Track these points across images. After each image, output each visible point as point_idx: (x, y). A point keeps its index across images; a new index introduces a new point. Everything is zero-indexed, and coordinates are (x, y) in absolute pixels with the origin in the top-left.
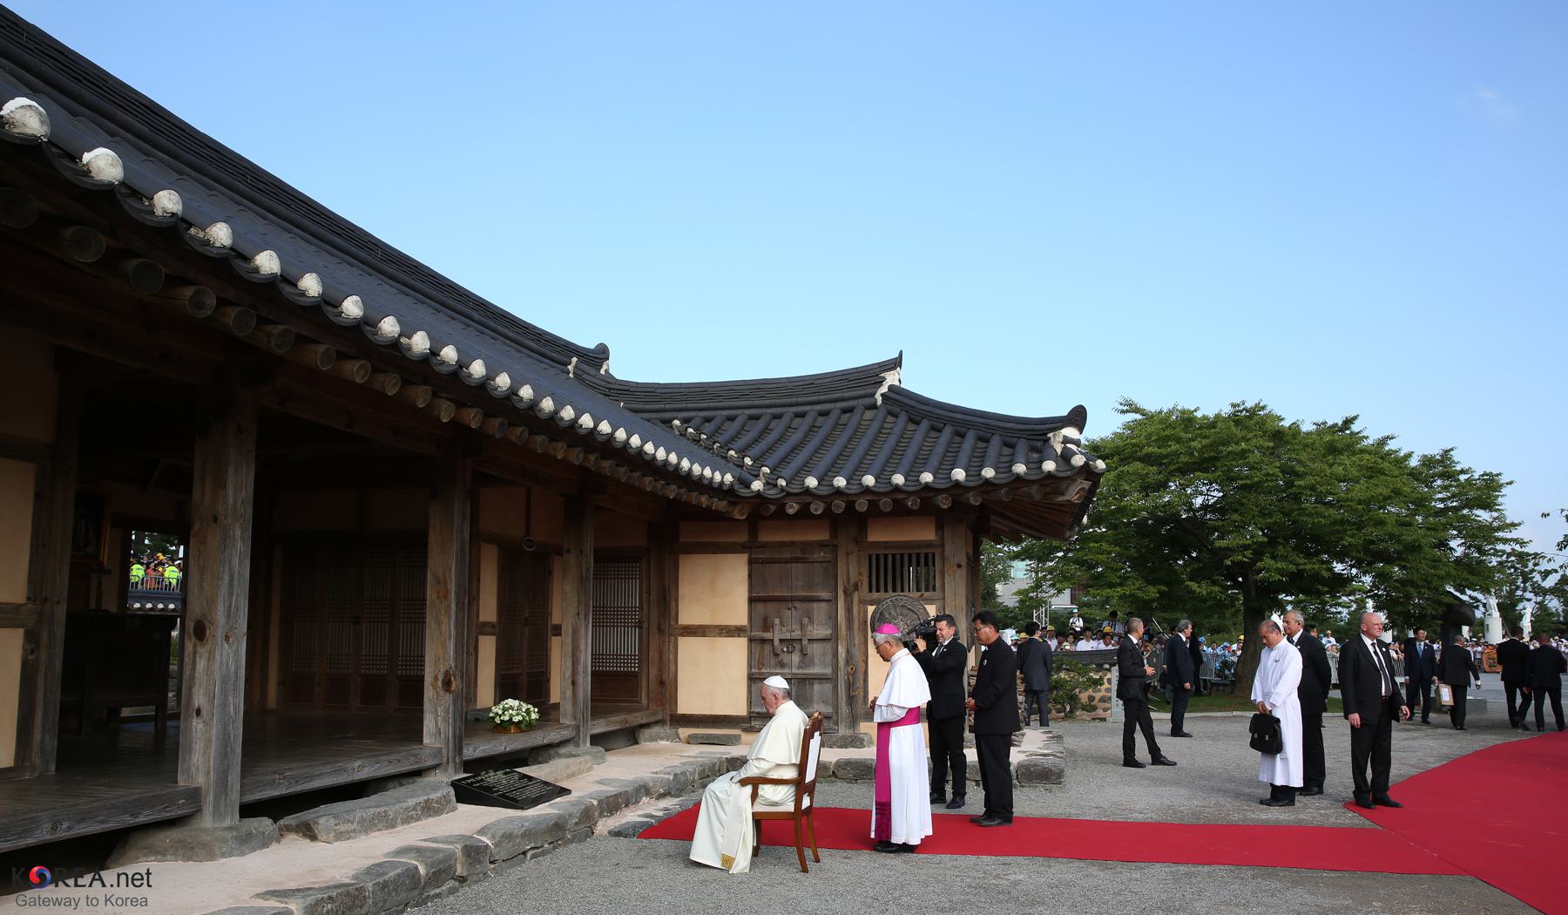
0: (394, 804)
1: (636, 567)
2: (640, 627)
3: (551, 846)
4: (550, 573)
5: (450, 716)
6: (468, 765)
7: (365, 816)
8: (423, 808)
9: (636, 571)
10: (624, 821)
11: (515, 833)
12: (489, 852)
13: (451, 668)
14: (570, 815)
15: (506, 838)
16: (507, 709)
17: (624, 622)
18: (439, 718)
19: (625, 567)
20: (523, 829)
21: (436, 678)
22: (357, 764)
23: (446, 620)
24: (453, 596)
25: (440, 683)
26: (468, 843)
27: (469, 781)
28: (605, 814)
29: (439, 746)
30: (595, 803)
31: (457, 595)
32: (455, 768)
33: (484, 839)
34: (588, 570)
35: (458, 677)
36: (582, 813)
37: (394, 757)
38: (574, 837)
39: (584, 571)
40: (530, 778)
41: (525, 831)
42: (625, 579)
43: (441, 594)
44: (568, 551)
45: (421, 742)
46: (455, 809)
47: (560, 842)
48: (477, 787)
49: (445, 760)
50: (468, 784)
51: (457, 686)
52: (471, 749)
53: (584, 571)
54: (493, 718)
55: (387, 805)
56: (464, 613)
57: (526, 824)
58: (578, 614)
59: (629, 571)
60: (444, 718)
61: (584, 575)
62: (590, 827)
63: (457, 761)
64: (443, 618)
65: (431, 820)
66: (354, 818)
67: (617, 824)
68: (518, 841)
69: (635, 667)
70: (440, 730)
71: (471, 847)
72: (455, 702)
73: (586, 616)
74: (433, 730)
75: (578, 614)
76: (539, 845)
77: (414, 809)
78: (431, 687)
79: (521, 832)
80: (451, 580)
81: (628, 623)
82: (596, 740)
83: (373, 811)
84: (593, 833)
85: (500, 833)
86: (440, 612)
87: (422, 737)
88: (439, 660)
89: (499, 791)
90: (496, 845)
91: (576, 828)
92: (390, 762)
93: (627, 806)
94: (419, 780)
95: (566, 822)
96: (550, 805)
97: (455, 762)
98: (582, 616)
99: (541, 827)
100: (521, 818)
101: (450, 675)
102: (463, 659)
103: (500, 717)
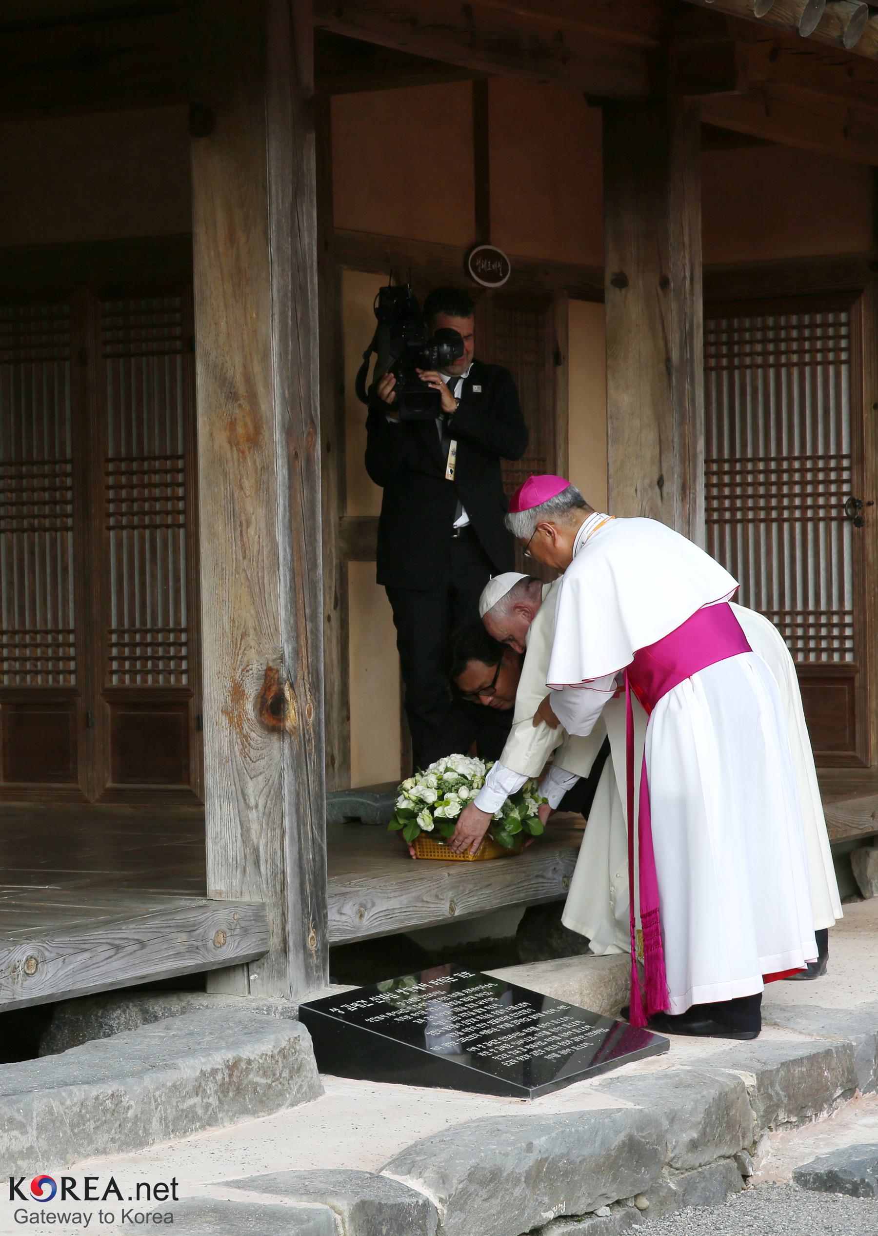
0: (138, 1074)
1: (837, 325)
2: (858, 522)
3: (619, 1213)
4: (559, 359)
5: (287, 806)
7: (55, 1104)
8: (223, 1089)
9: (837, 337)
10: (845, 1140)
11: (509, 1166)
12: (431, 1225)
13: (282, 658)
14: (673, 1118)
15: (483, 1183)
16: (454, 788)
17: (804, 508)
18: (253, 815)
19: (800, 327)
20: (531, 1160)
21: (237, 693)
22: (22, 952)
23: (261, 512)
24: (278, 436)
25: (249, 707)
26: (369, 1195)
27: (353, 1007)
28: (782, 1116)
29: (257, 899)
30: (750, 1080)
31: (289, 431)
32: (308, 969)
33: (414, 1183)
34: (687, 338)
35: (304, 688)
36: (708, 1113)
37: (129, 931)
38: (688, 1187)
39: (675, 338)
40: (536, 1001)
41: (540, 1163)
42: (801, 365)
43: (240, 431)
44: (621, 281)
45: (199, 887)
46: (314, 1092)
47: (644, 1202)
49: (274, 942)
50: (348, 1015)
51: (300, 714)
52: (350, 909)
53: (675, 338)
54: (411, 815)
55: (119, 1076)
56: (313, 489)
57: (541, 1142)
58: (660, 483)
59: (813, 338)
60: (268, 815)
61: (675, 356)
62: (736, 1157)
63: (313, 945)
65: (247, 1123)
66: (28, 1113)
67: (824, 1151)
68: (517, 1192)
69: (842, 651)
70: (256, 850)
71: (380, 1208)
72: (298, 766)
73: (685, 489)
74: (236, 849)
75: (660, 483)
76: (580, 1209)
77: (198, 1090)
78: (224, 721)
79: (523, 1168)
80: (268, 385)
81: (816, 507)
83: (79, 1093)
84: (745, 1177)
85: (460, 1169)
86: (241, 488)
87: (203, 874)
88: (244, 635)
90: (456, 1203)
91: (693, 1159)
92: (118, 948)
93: (849, 1092)
94: (198, 1000)
95: (661, 1138)
96: (609, 1085)
97: (305, 947)
98: (673, 487)
99: (586, 1152)
100: (523, 1122)
101: (280, 683)
102: (315, 632)
103: (432, 809)
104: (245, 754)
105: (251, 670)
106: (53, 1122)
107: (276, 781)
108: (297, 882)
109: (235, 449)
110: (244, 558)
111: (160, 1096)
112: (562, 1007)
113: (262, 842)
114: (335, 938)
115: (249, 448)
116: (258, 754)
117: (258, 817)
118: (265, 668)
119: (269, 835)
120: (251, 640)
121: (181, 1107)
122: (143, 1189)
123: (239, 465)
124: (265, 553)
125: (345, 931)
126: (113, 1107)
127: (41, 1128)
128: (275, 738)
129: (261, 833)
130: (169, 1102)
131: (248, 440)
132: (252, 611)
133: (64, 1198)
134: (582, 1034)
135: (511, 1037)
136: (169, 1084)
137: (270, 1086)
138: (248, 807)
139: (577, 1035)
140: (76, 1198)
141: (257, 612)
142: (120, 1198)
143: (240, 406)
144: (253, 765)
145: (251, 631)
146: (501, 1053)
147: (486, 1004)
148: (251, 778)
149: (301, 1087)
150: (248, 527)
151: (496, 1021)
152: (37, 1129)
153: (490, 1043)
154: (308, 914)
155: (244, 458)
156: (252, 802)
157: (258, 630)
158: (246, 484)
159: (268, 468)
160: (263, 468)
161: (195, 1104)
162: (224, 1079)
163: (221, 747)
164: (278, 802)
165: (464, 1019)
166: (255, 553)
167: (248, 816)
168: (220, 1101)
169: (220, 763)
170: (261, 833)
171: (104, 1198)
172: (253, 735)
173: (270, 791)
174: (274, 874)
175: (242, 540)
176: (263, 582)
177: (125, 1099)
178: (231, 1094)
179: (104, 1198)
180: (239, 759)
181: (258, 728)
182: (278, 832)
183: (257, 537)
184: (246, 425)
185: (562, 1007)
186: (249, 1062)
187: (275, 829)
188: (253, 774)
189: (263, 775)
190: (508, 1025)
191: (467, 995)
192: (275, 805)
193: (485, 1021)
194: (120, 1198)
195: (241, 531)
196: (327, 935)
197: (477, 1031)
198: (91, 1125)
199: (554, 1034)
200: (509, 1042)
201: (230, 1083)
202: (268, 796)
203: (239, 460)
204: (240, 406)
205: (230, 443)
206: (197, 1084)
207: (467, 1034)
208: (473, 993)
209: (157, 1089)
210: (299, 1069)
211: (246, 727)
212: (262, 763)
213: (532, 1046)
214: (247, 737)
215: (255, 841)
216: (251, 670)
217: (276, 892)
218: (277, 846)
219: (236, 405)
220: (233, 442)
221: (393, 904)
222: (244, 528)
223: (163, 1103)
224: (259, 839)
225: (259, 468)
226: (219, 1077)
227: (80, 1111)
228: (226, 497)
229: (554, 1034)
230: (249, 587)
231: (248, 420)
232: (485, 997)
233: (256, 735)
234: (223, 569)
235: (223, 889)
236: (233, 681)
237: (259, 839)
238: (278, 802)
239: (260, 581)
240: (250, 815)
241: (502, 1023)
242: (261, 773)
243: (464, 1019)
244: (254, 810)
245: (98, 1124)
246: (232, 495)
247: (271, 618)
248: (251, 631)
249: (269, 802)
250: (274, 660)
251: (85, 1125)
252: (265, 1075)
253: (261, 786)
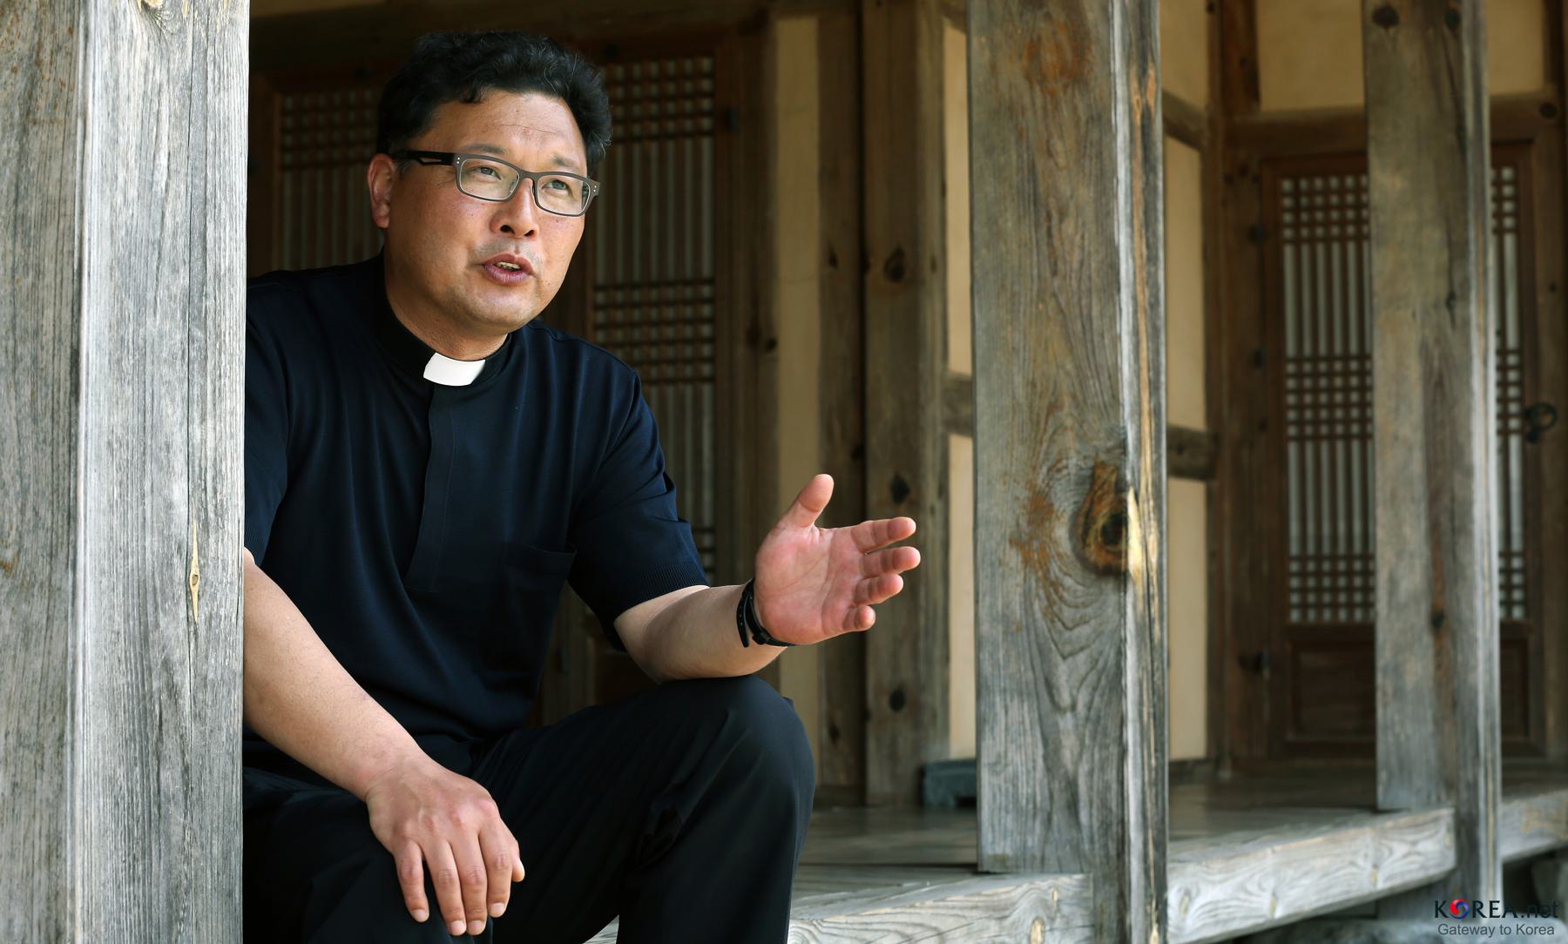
18: (1066, 722)
23: (1086, 194)
25: (1061, 531)
43: (1048, 57)
64: (1065, 189)
70: (1072, 785)
86: (1050, 153)
88: (1054, 407)
104: (1052, 615)
105: (1066, 467)
107: (1112, 661)
109: (1037, 88)
110: (1054, 273)
113: (1084, 769)
115: (1066, 87)
116: (1078, 616)
117: (1076, 726)
118: (1090, 463)
119: (1097, 756)
120: (1067, 416)
123: (1046, 116)
124: (1093, 265)
129: (1081, 754)
131: (1062, 73)
132: (1069, 366)
138: (1057, 707)
141: (1078, 368)
143: (1048, 16)
144: (1067, 634)
145: (1067, 401)
148: (1064, 658)
150: (1061, 221)
154: (1151, 896)
155: (1056, 107)
156: (1065, 699)
157: (1080, 397)
158: (1059, 146)
159: (1100, 117)
160: (1090, 119)
163: (1007, 605)
164: (1114, 699)
166: (1076, 266)
167: (1056, 724)
169: (1005, 633)
170: (1081, 754)
172: (1068, 582)
173: (1099, 680)
174: (1105, 826)
175: (1050, 244)
176: (1090, 315)
180: (1042, 624)
181: (1077, 569)
182: (1114, 750)
183: (1078, 238)
184: (1058, 48)
187: (1107, 747)
188: (1067, 649)
189: (1087, 651)
192: (1109, 703)
195: (1049, 229)
202: (1095, 689)
203: (1045, 109)
204: (1048, 16)
205: (1028, 77)
211: (1055, 568)
212: (1084, 631)
214: (1055, 585)
215: (1070, 767)
216: (1066, 467)
217: (1107, 856)
218: (1112, 775)
219: (1040, 14)
220: (1035, 75)
222: (1055, 221)
224: (1076, 764)
225: (1083, 119)
228: (1020, 169)
230: (1065, 325)
231: (1063, 38)
233: (1073, 583)
234: (1013, 295)
235: (1009, 852)
236: (1031, 485)
237: (1076, 764)
238: (1114, 699)
239: (1085, 312)
240: (1062, 724)
242: (1082, 649)
244: (1069, 715)
246: (1032, 168)
247: (1104, 377)
248: (1067, 401)
249: (1097, 699)
250: (1109, 451)
253: (1083, 671)
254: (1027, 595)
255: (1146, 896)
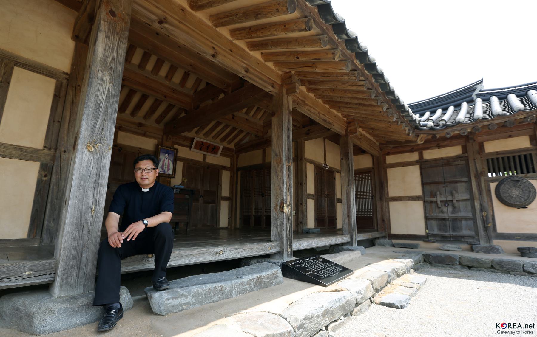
6: (296, 253)
18: (278, 227)
21: (277, 205)
23: (281, 174)
25: (278, 208)
48: (297, 268)
51: (288, 209)
60: (281, 227)
70: (279, 233)
74: (275, 233)
77: (248, 283)
78: (274, 210)
80: (283, 153)
82: (360, 243)
86: (278, 170)
88: (278, 195)
89: (310, 271)
97: (287, 251)
104: (277, 216)
106: (199, 294)
108: (286, 239)
111: (236, 286)
112: (334, 264)
113: (280, 231)
114: (293, 250)
121: (242, 288)
122: (527, 326)
125: (297, 248)
126: (220, 289)
127: (193, 296)
128: (282, 213)
130: (239, 287)
133: (508, 328)
134: (338, 270)
135: (324, 271)
136: (239, 283)
137: (269, 282)
138: (278, 225)
139: (337, 270)
140: (511, 328)
142: (521, 328)
146: (321, 274)
147: (320, 263)
149: (277, 281)
151: (321, 267)
152: (192, 296)
153: (319, 272)
156: (278, 225)
158: (279, 170)
161: (247, 287)
162: (256, 281)
165: (315, 266)
168: (254, 286)
171: (518, 328)
174: (282, 237)
177: (225, 287)
178: (258, 284)
179: (518, 328)
180: (277, 217)
185: (334, 264)
186: (264, 276)
190: (324, 268)
191: (317, 261)
193: (319, 267)
194: (521, 328)
196: (292, 249)
197: (317, 269)
198: (212, 294)
199: (333, 270)
200: (323, 272)
201: (258, 281)
206: (248, 282)
207: (315, 270)
208: (318, 261)
209: (236, 284)
210: (277, 278)
213: (328, 273)
214: (278, 213)
218: (282, 232)
221: (306, 244)
223: (237, 287)
226: (255, 280)
227: (209, 291)
229: (333, 270)
232: (320, 261)
233: (279, 213)
236: (276, 203)
241: (323, 267)
243: (315, 266)
245: (214, 294)
251: (210, 294)
252: (268, 279)
254: (275, 214)
255: (287, 245)
